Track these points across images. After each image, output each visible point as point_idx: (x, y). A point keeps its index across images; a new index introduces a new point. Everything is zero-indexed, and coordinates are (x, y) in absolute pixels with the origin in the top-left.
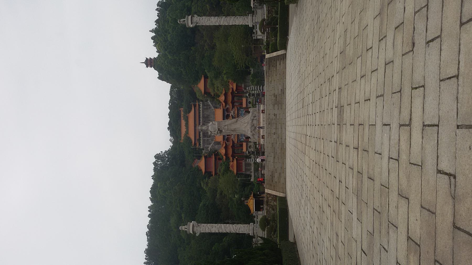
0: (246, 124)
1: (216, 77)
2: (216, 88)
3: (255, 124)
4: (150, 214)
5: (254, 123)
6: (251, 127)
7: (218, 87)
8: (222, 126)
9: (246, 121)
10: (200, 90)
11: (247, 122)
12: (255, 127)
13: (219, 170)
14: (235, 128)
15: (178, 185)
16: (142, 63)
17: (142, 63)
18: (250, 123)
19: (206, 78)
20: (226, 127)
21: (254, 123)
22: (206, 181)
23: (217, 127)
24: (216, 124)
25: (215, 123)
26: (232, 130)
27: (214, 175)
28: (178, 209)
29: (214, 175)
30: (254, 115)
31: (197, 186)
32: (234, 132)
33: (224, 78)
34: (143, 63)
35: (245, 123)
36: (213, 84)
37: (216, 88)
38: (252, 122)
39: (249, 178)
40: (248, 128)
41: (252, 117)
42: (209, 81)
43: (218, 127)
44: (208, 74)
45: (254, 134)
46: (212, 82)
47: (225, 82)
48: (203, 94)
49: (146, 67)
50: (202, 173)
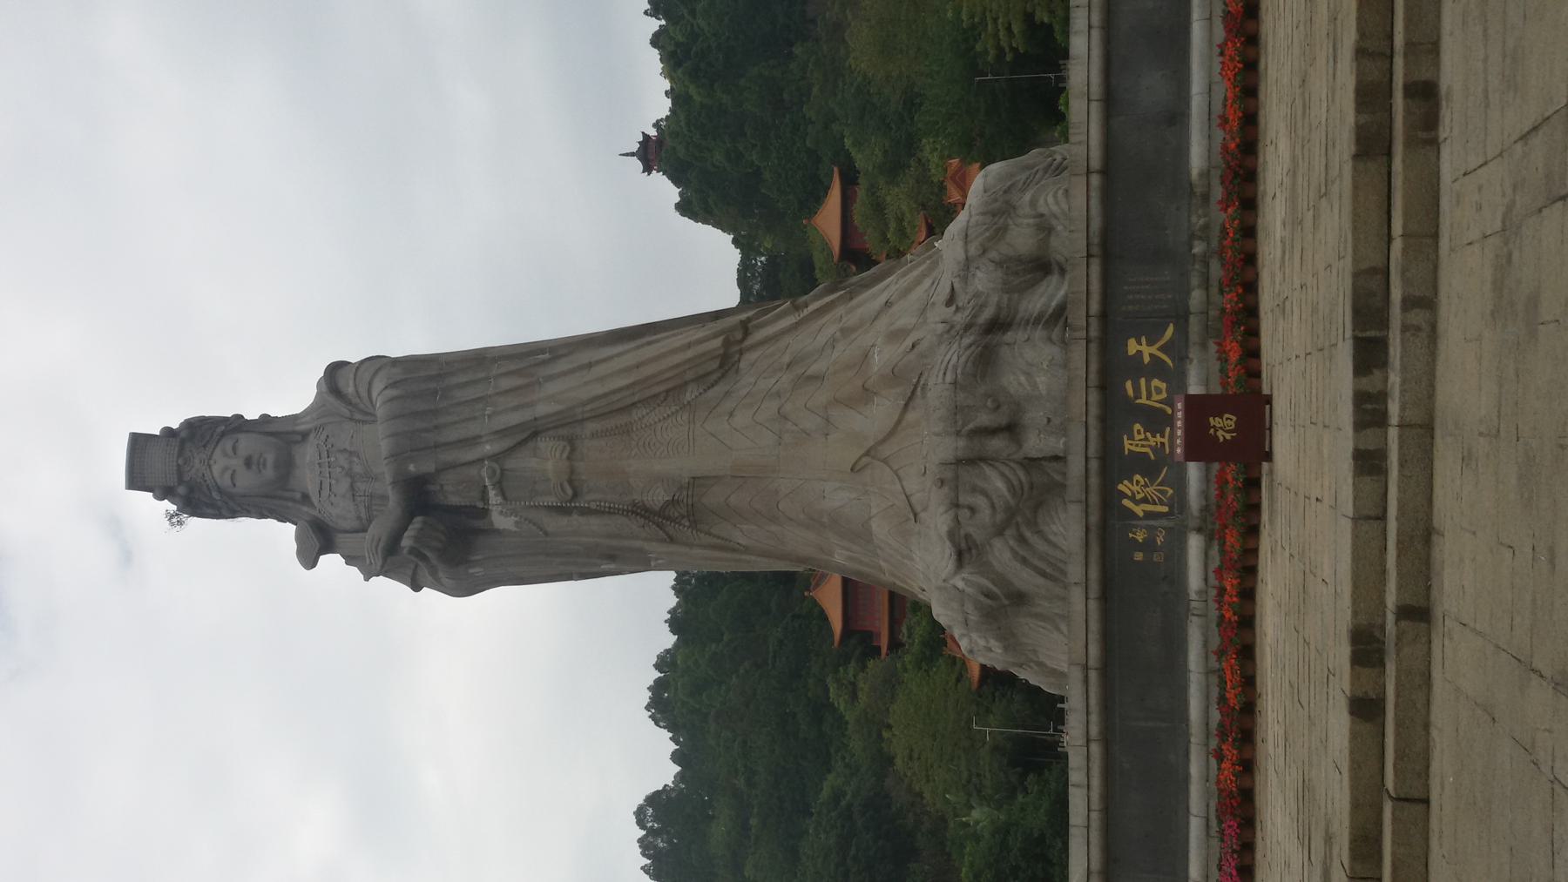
0: (881, 412)
1: (893, 168)
2: (893, 225)
3: (1035, 416)
4: (676, 750)
5: (1013, 381)
6: (959, 462)
7: (900, 220)
8: (472, 441)
9: (883, 357)
10: (826, 246)
11: (894, 376)
12: (1030, 463)
13: (910, 629)
14: (696, 481)
15: (742, 671)
16: (627, 155)
17: (627, 155)
18: (937, 390)
19: (849, 181)
20: (546, 460)
21: (1013, 381)
22: (851, 675)
23: (385, 446)
24: (380, 411)
25: (363, 392)
26: (640, 511)
27: (884, 650)
28: (740, 782)
29: (884, 650)
30: (1021, 239)
31: (810, 695)
32: (672, 540)
33: (929, 170)
34: (632, 154)
35: (866, 395)
36: (878, 208)
37: (893, 225)
38: (985, 361)
39: (1051, 732)
40: (912, 485)
41: (984, 280)
42: (861, 192)
43: (397, 456)
44: (860, 160)
45: (1019, 598)
46: (873, 194)
47: (936, 190)
48: (836, 259)
49: (643, 172)
50: (832, 635)
